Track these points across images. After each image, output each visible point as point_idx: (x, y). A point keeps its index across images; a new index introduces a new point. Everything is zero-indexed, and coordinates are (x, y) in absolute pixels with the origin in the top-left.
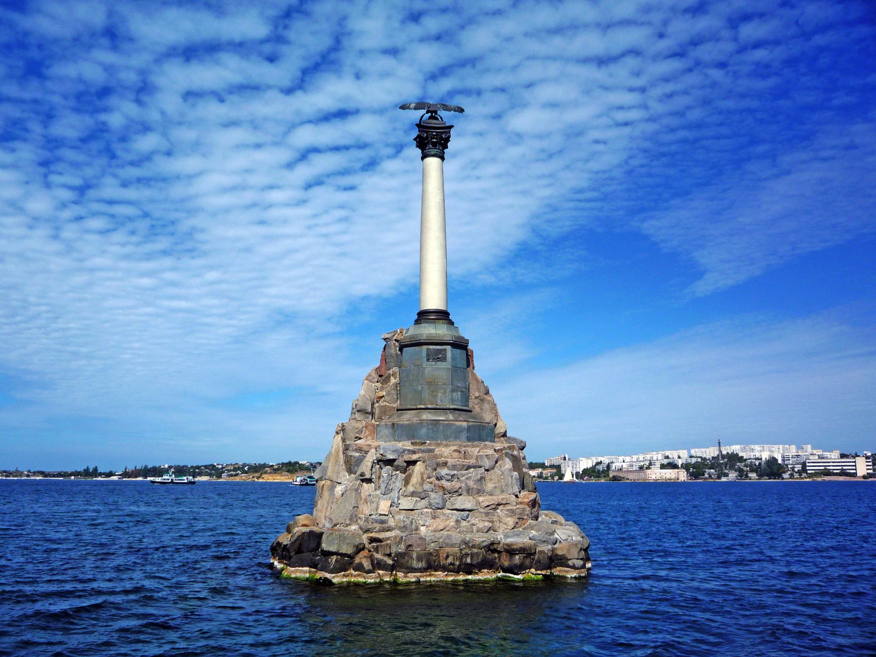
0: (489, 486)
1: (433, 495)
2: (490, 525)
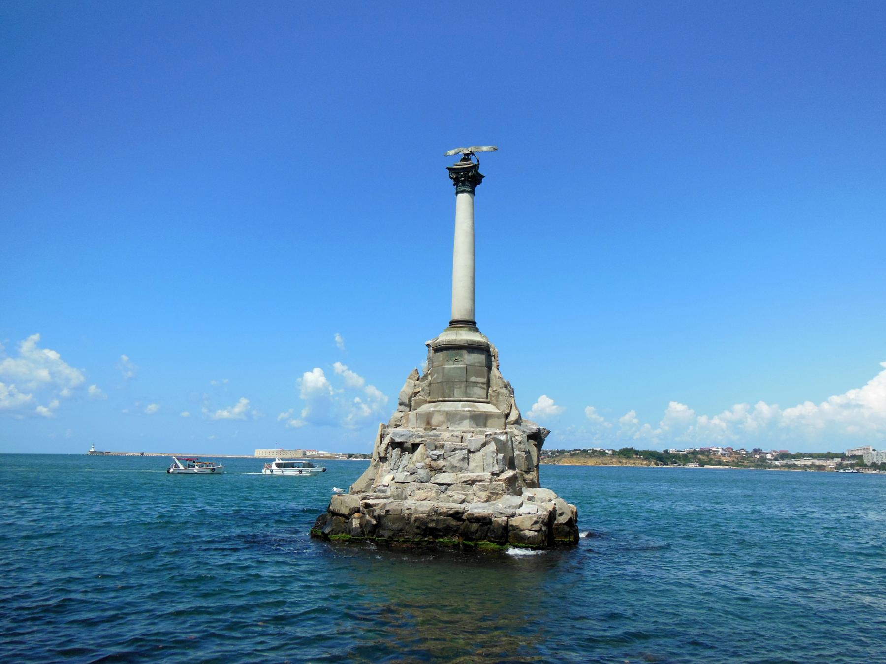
0: (472, 465)
1: (420, 471)
2: (464, 497)
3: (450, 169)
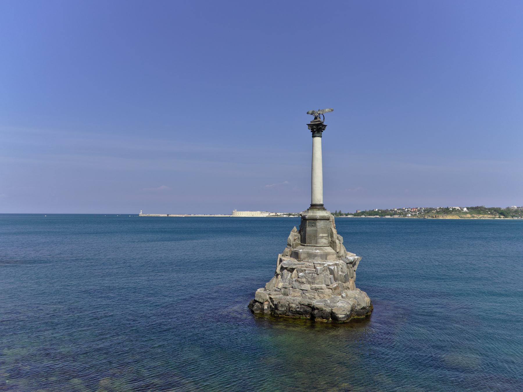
0: (317, 281)
3: (308, 125)
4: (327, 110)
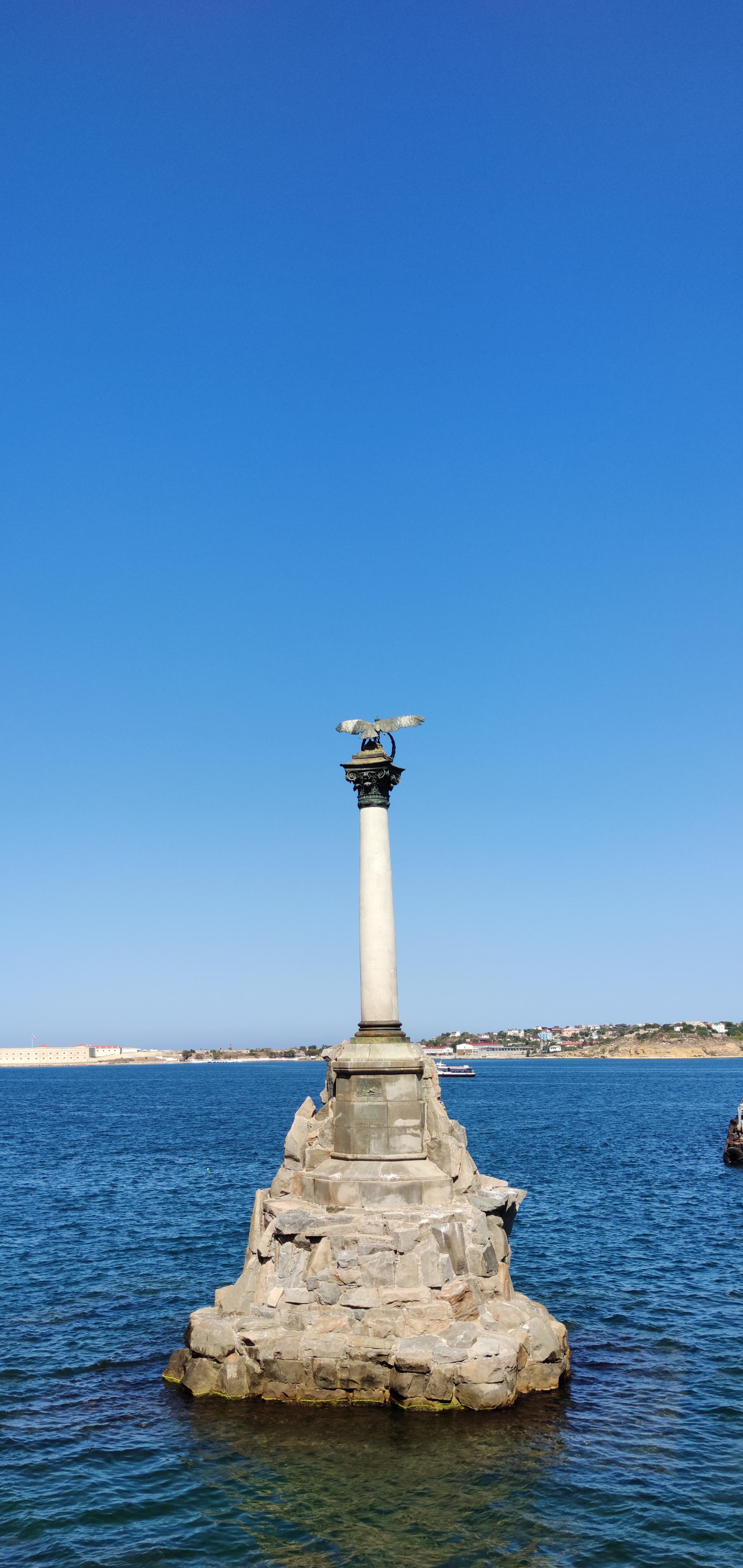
0: (401, 1274)
4: (405, 721)
